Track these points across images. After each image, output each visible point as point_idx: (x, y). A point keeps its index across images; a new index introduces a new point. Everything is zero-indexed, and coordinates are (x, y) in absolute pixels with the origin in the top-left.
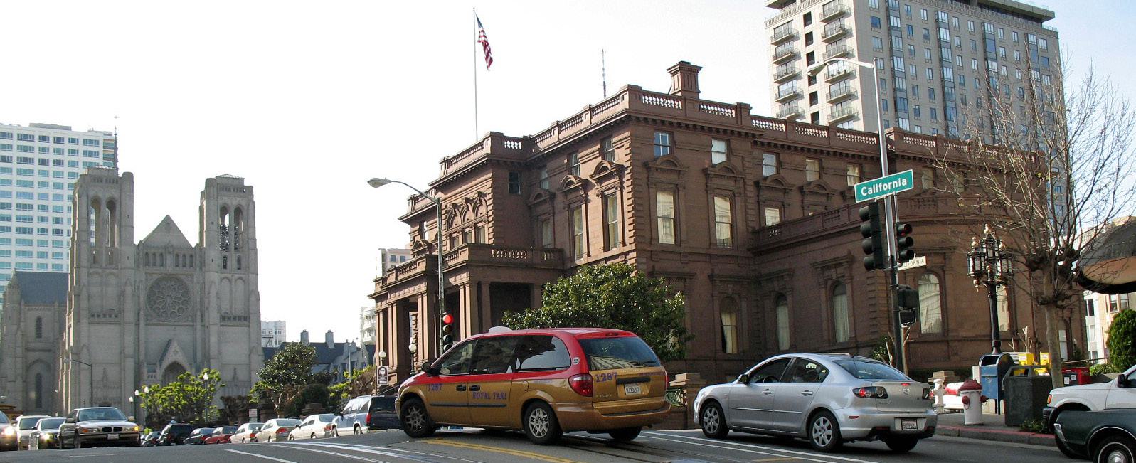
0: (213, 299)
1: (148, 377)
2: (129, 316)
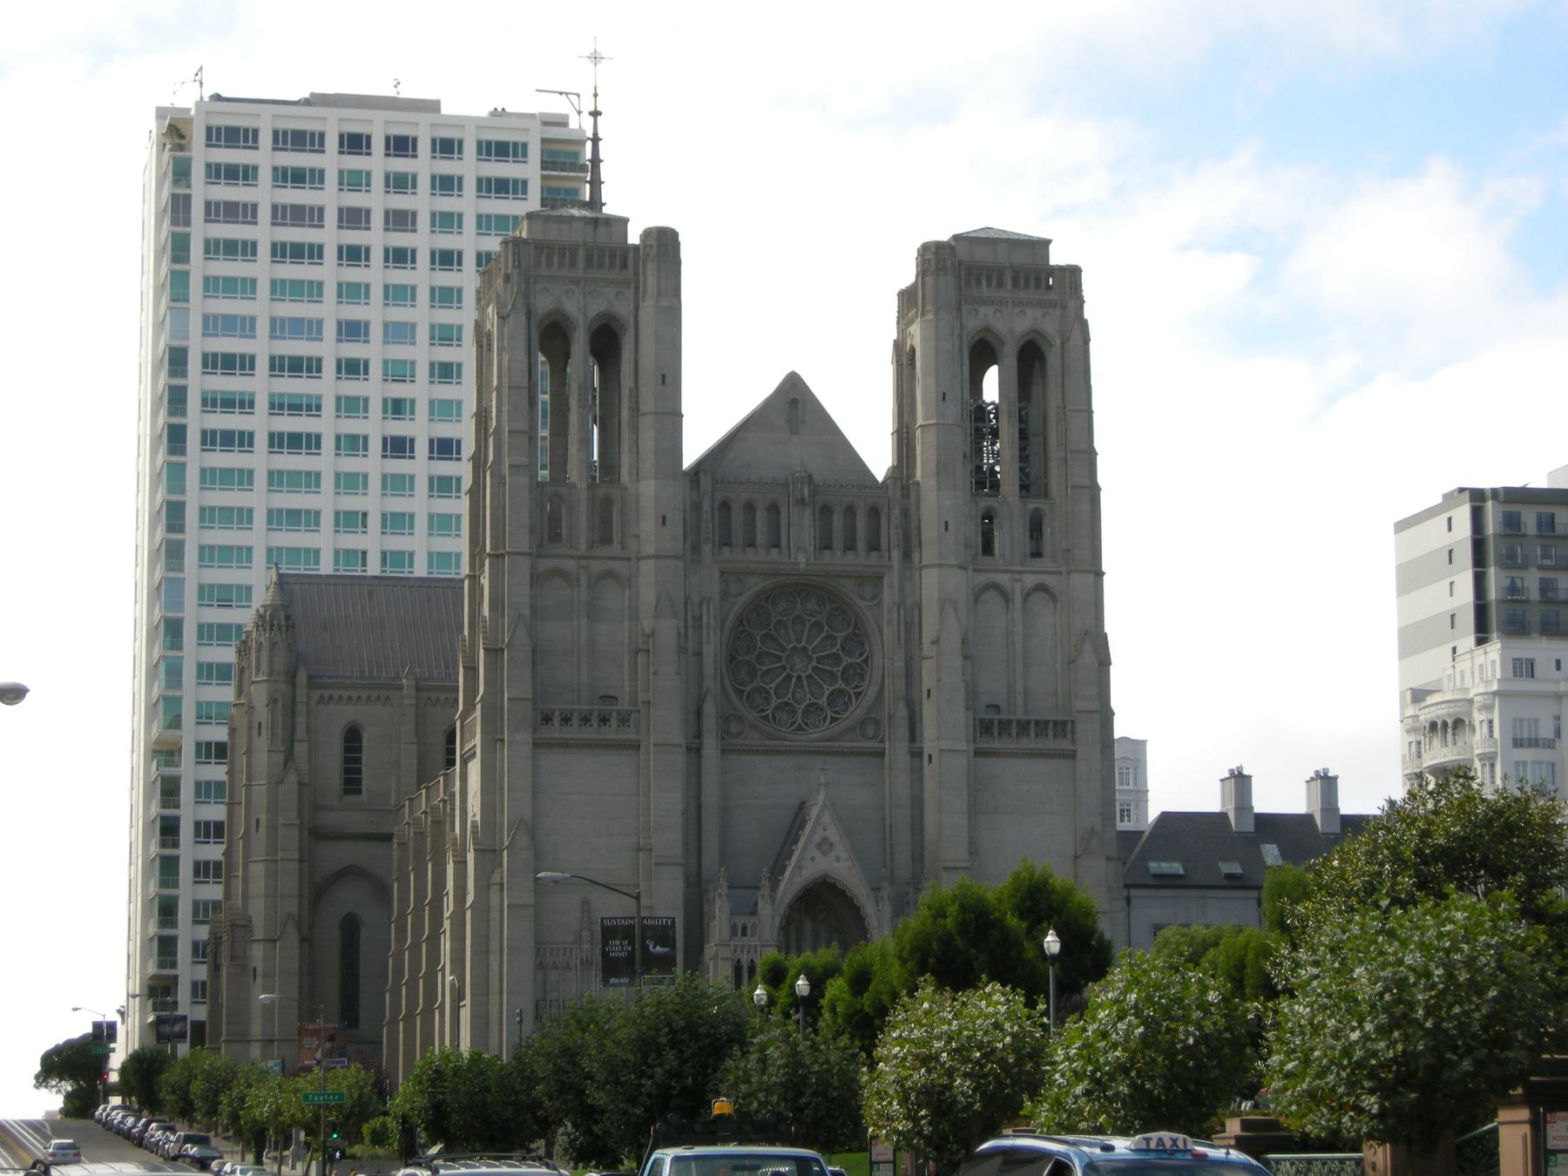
2: (667, 723)
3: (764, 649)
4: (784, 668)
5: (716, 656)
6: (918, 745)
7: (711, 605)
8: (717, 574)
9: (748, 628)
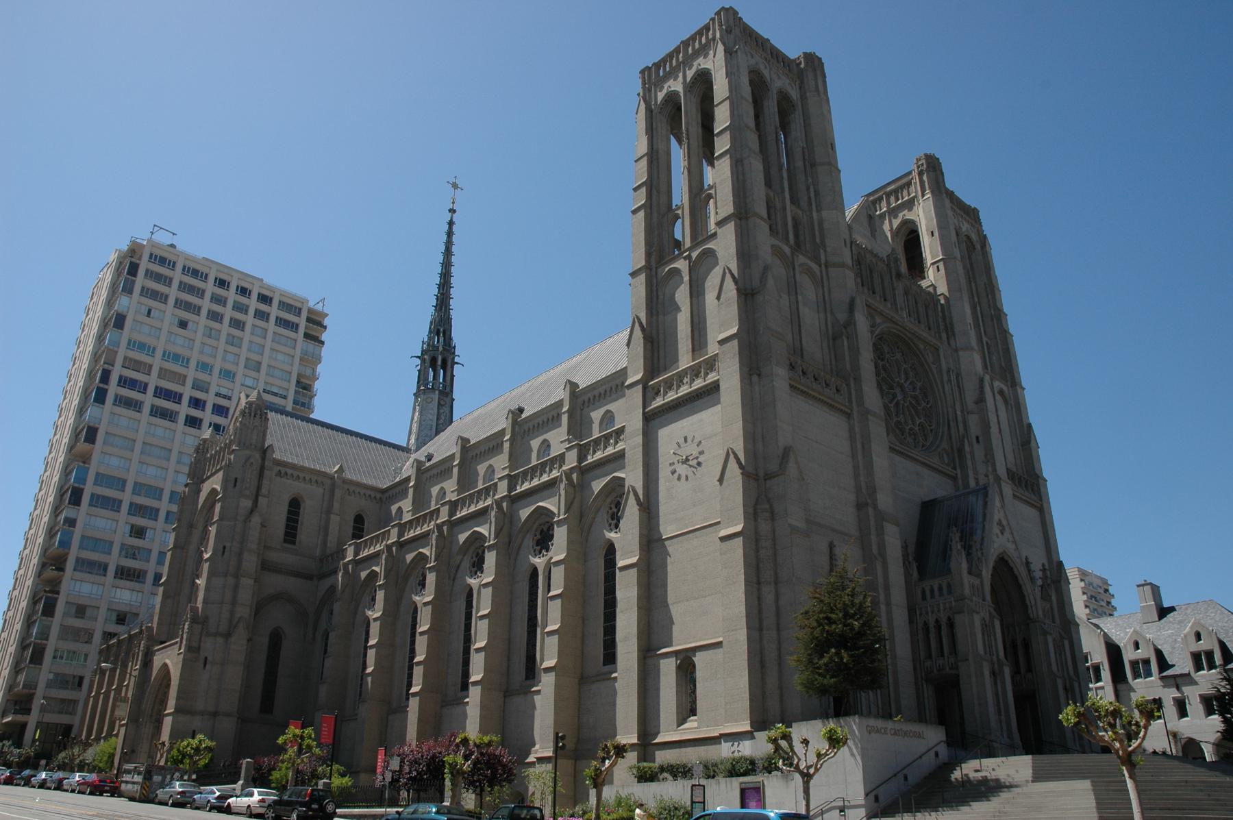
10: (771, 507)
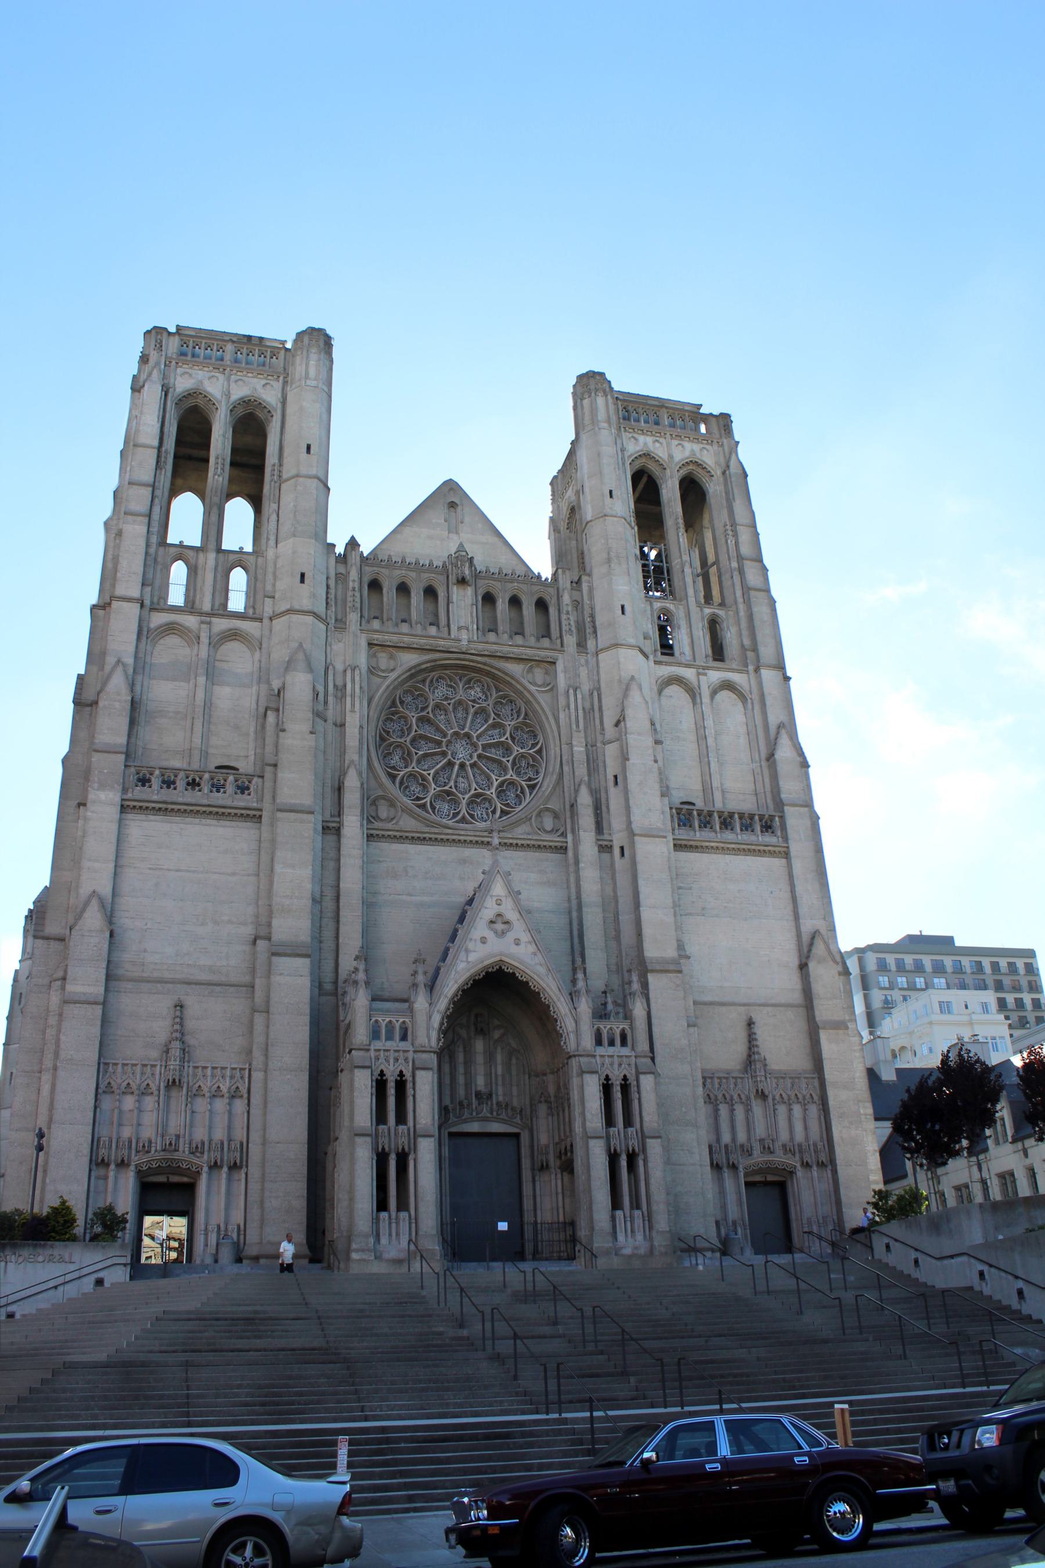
0: (639, 741)
1: (375, 1034)
3: (420, 732)
4: (444, 754)
5: (361, 727)
6: (606, 837)
7: (357, 672)
8: (364, 643)
9: (401, 709)
10: (66, 972)
